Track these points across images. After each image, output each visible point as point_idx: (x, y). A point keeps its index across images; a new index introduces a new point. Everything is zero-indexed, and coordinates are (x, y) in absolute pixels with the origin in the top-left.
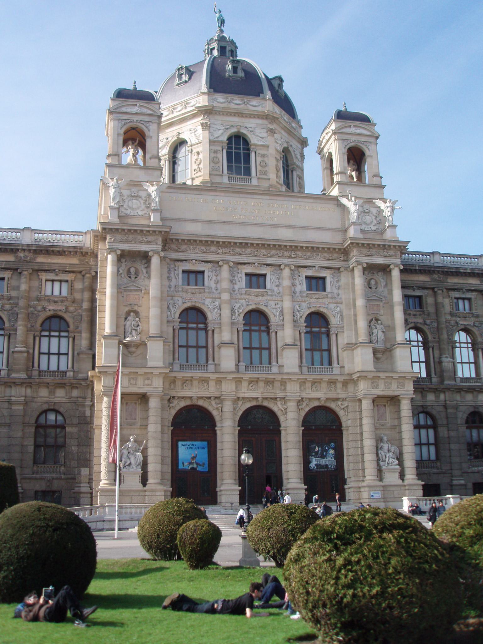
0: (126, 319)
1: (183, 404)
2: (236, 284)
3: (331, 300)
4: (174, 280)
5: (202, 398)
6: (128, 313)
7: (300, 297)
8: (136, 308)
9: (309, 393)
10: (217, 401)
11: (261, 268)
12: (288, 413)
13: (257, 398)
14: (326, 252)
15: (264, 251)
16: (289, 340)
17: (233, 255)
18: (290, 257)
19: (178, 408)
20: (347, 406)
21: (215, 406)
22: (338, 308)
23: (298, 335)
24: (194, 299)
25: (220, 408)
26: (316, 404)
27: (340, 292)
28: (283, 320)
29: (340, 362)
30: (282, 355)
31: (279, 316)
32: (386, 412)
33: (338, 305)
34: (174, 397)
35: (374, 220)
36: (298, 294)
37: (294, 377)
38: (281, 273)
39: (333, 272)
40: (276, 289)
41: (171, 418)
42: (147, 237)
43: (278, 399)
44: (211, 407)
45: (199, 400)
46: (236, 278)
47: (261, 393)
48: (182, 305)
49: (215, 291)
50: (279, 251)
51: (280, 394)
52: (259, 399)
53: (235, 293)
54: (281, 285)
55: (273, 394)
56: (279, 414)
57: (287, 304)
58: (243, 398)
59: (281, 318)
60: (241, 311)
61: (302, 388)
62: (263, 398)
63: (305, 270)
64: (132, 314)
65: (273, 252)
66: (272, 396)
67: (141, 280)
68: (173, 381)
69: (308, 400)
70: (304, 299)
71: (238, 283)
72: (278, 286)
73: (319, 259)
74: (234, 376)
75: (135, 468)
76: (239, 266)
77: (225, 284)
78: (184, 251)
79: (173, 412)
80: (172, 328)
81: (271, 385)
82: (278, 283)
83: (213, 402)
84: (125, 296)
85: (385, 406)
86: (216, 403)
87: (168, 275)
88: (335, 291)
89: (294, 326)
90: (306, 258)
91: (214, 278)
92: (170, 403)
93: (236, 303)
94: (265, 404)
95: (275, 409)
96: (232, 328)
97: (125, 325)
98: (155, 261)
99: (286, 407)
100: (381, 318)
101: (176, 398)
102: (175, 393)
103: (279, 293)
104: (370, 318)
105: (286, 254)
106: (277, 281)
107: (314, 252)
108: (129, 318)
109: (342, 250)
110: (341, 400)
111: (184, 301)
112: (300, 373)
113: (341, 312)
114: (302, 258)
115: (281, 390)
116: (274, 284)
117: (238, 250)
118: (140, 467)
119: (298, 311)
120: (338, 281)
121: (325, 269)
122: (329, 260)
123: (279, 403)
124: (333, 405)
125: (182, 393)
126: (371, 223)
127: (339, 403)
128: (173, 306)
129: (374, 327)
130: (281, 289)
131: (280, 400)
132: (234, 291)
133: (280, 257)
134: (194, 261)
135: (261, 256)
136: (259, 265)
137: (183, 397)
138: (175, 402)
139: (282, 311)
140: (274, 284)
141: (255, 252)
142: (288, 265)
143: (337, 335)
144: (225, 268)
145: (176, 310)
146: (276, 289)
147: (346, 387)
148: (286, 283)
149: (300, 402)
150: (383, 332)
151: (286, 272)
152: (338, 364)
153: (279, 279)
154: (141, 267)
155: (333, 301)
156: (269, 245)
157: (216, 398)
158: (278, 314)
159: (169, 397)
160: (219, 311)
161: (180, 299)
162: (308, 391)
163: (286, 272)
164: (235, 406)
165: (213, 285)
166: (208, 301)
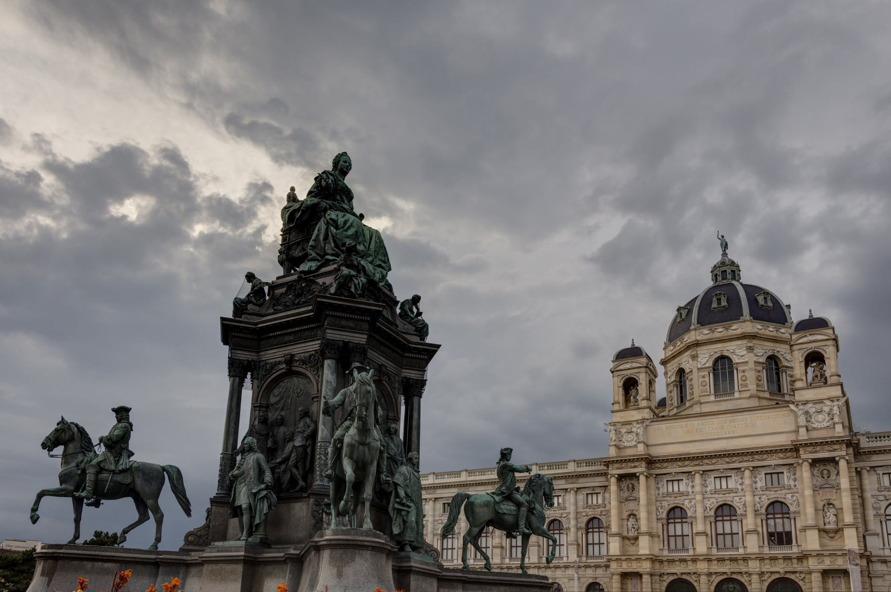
0: (628, 520)
1: (672, 578)
2: (707, 487)
3: (788, 491)
4: (661, 489)
5: (684, 573)
6: (630, 515)
7: (760, 492)
8: (634, 512)
9: (767, 567)
10: (696, 575)
12: (752, 584)
13: (726, 573)
14: (779, 452)
15: (727, 460)
16: (751, 527)
17: (702, 465)
19: (668, 581)
20: (804, 578)
24: (676, 502)
25: (698, 581)
26: (778, 576)
27: (796, 483)
28: (746, 511)
29: (798, 542)
30: (746, 539)
31: (742, 508)
32: (841, 583)
33: (794, 494)
34: (663, 574)
35: (827, 417)
36: (759, 489)
37: (753, 556)
38: (744, 474)
40: (740, 487)
42: (635, 463)
43: (743, 573)
44: (692, 579)
45: (683, 575)
46: (707, 482)
48: (667, 505)
49: (691, 494)
51: (744, 569)
53: (708, 493)
54: (744, 484)
55: (738, 569)
56: (746, 584)
57: (748, 498)
58: (715, 573)
59: (745, 509)
60: (711, 507)
61: (763, 564)
62: (732, 573)
63: (763, 469)
64: (632, 516)
65: (735, 459)
66: (738, 570)
67: (636, 492)
68: (661, 562)
69: (769, 573)
70: (764, 493)
71: (709, 485)
72: (741, 484)
73: (774, 459)
74: (704, 557)
76: (708, 473)
77: (698, 488)
78: (666, 468)
79: (665, 584)
81: (736, 563)
82: (741, 482)
83: (693, 576)
84: (626, 504)
85: (840, 577)
86: (695, 577)
87: (656, 486)
88: (792, 483)
89: (755, 515)
90: (763, 460)
91: (691, 484)
93: (708, 501)
94: (734, 576)
95: (742, 580)
96: (705, 520)
97: (627, 525)
98: (642, 479)
100: (834, 502)
103: (742, 490)
104: (822, 503)
105: (745, 458)
106: (740, 480)
108: (631, 520)
109: (794, 449)
110: (799, 572)
111: (669, 503)
114: (759, 460)
115: (745, 566)
116: (738, 483)
117: (706, 461)
119: (759, 503)
120: (794, 474)
121: (781, 466)
122: (782, 458)
124: (792, 577)
126: (824, 420)
127: (798, 575)
128: (661, 508)
129: (827, 511)
130: (744, 487)
132: (706, 492)
133: (740, 462)
134: (673, 474)
136: (724, 470)
137: (671, 573)
138: (666, 577)
139: (745, 504)
140: (738, 483)
143: (795, 519)
144: (697, 476)
146: (740, 487)
147: (802, 562)
148: (747, 481)
150: (835, 515)
151: (747, 473)
152: (797, 543)
153: (742, 478)
154: (635, 483)
156: (729, 454)
157: (694, 573)
158: (741, 507)
160: (695, 509)
162: (768, 566)
163: (747, 473)
165: (690, 490)
166: (686, 502)
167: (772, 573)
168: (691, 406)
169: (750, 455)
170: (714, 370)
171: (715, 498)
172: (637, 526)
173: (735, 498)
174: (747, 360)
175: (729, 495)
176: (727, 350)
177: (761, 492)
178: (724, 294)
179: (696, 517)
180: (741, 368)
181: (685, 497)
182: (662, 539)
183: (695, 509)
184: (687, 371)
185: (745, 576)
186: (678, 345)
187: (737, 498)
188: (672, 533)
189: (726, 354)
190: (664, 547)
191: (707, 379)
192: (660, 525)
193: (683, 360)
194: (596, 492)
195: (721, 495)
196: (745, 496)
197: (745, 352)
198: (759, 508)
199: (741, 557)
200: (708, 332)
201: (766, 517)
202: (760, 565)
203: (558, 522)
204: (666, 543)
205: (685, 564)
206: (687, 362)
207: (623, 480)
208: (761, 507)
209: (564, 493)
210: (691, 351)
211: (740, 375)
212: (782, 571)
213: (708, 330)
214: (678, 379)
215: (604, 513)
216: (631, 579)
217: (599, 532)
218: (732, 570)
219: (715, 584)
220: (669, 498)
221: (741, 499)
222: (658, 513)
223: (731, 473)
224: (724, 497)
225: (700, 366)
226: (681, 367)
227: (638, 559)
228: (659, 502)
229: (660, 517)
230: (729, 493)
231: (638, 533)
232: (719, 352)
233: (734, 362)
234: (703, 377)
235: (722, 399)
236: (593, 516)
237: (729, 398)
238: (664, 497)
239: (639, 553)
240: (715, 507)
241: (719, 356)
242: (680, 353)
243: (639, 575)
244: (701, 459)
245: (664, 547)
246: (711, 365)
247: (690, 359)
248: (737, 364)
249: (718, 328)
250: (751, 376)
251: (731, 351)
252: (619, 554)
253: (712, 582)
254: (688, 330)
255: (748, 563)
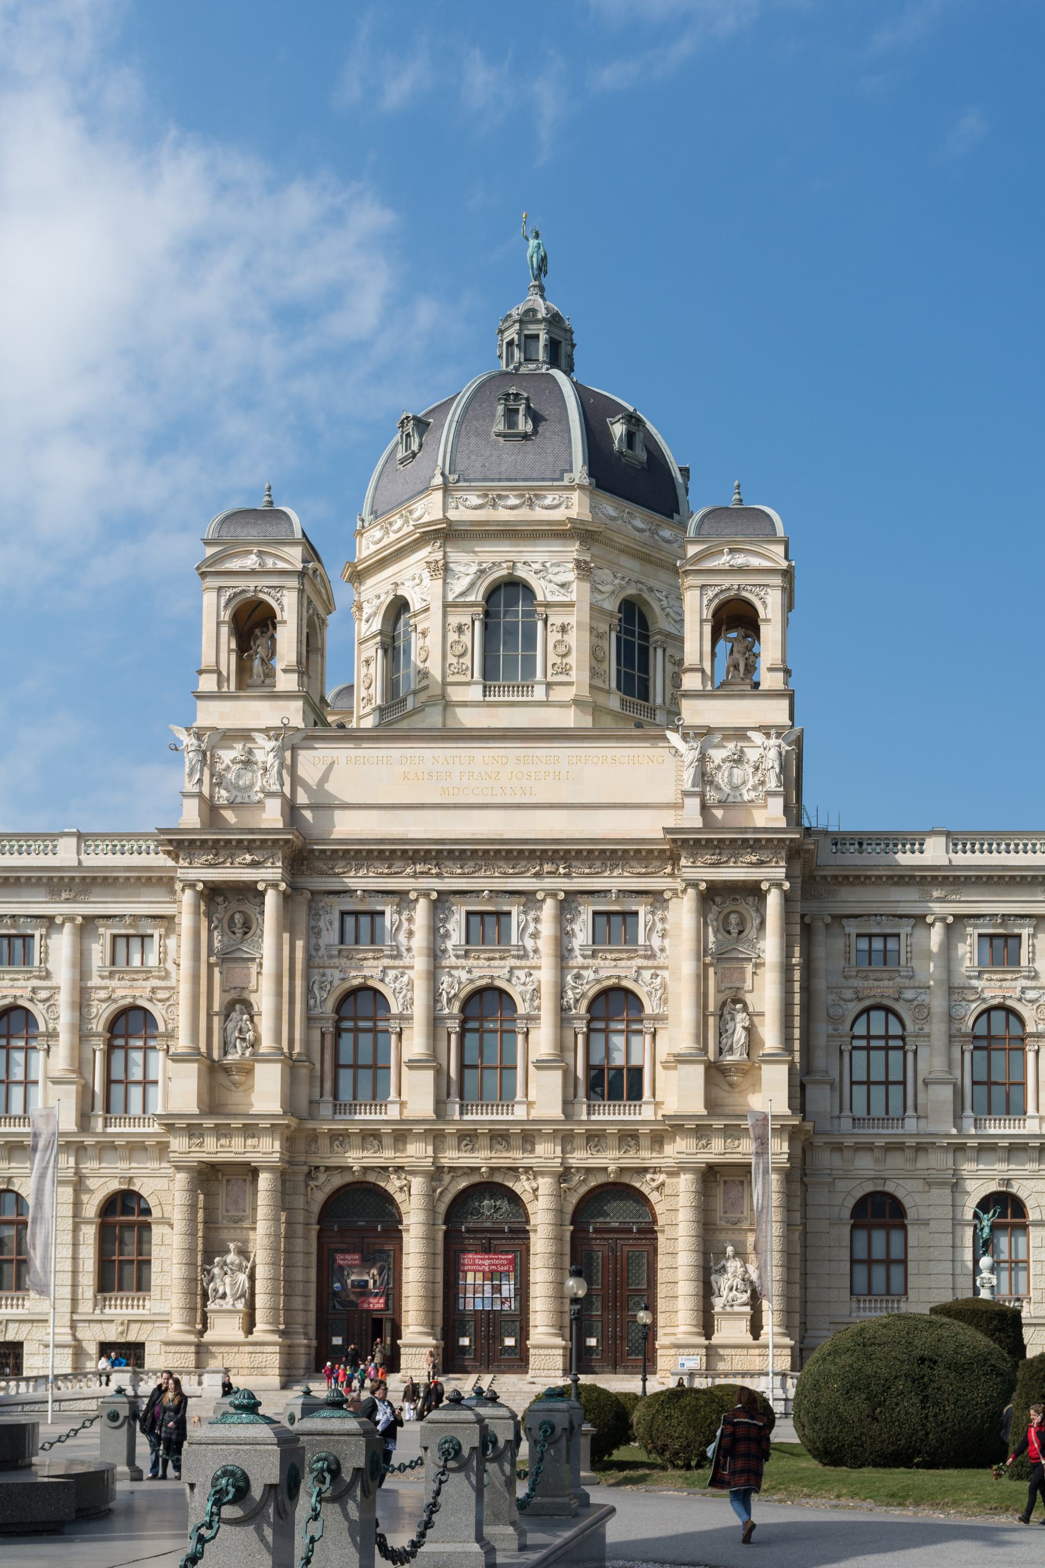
1: (337, 1181)
9: (579, 1158)
11: (499, 899)
12: (540, 1198)
13: (480, 1168)
18: (552, 874)
19: (328, 1189)
21: (398, 1184)
22: (659, 980)
23: (573, 1038)
25: (406, 1189)
26: (601, 1179)
28: (539, 1008)
31: (532, 1000)
34: (317, 1168)
36: (577, 952)
39: (651, 900)
41: (316, 1208)
43: (520, 1170)
44: (392, 1185)
47: (486, 1159)
50: (533, 862)
52: (483, 1170)
56: (526, 1198)
58: (452, 1169)
59: (536, 1004)
60: (453, 992)
61: (569, 1148)
68: (314, 1137)
71: (452, 932)
75: (231, 1302)
77: (420, 940)
79: (320, 1197)
80: (319, 1032)
92: (313, 1179)
94: (498, 1179)
99: (535, 1185)
101: (322, 1169)
102: (318, 1160)
105: (547, 867)
106: (532, 925)
107: (609, 859)
112: (562, 1117)
113: (664, 986)
115: (524, 1151)
118: (243, 1300)
123: (523, 1177)
125: (332, 1160)
127: (649, 1176)
128: (321, 988)
131: (526, 1172)
135: (497, 874)
136: (493, 894)
138: (322, 1177)
139: (537, 991)
141: (484, 868)
142: (552, 894)
145: (325, 995)
146: (529, 944)
149: (564, 1174)
155: (650, 963)
158: (528, 996)
159: (305, 1169)
161: (336, 972)
164: (433, 1183)
167: (589, 1170)
168: (416, 711)
169: (562, 858)
170: (487, 614)
171: (463, 968)
172: (251, 1033)
173: (517, 972)
174: (574, 597)
175: (502, 963)
176: (524, 563)
177: (579, 961)
178: (527, 399)
179: (410, 1018)
180: (556, 619)
181: (386, 962)
182: (319, 1074)
183: (409, 995)
184: (415, 605)
185: (523, 1177)
186: (395, 527)
187: (521, 974)
188: (346, 1058)
189: (521, 573)
190: (322, 1096)
191: (466, 638)
192: (316, 1035)
193: (407, 574)
194: (141, 932)
195: (482, 962)
196: (539, 968)
197: (571, 576)
198: (572, 1001)
199: (516, 1129)
200: (480, 501)
201: (588, 1027)
202: (563, 1152)
203: (22, 1013)
204: (328, 1086)
205: (376, 1142)
206: (417, 581)
207: (220, 900)
208: (577, 1001)
209: (44, 931)
210: (429, 549)
211: (554, 637)
212: (612, 1168)
213: (479, 496)
214: (390, 629)
215: (162, 995)
216: (228, 1181)
217: (146, 1049)
218: (495, 1163)
219: (448, 1198)
220: (343, 961)
221: (531, 975)
222: (312, 1002)
223: (512, 904)
224: (489, 966)
225: (450, 598)
226: (399, 593)
227: (250, 1131)
228: (316, 971)
229: (317, 1012)
230: (502, 958)
231: (253, 1054)
232: (504, 565)
233: (540, 597)
234: (460, 629)
235: (502, 699)
236: (128, 1001)
237: (520, 699)
238: (331, 957)
239: (254, 1110)
240: (462, 995)
241: (503, 576)
242: (400, 554)
243: (253, 1172)
244: (435, 858)
245: (322, 1096)
246: (480, 598)
247: (426, 574)
248: (547, 605)
249: (508, 496)
250: (577, 641)
251: (537, 566)
252: (196, 1111)
253: (441, 1193)
254: (426, 489)
255: (533, 1144)
